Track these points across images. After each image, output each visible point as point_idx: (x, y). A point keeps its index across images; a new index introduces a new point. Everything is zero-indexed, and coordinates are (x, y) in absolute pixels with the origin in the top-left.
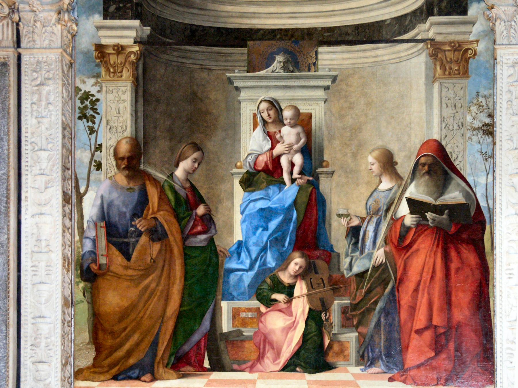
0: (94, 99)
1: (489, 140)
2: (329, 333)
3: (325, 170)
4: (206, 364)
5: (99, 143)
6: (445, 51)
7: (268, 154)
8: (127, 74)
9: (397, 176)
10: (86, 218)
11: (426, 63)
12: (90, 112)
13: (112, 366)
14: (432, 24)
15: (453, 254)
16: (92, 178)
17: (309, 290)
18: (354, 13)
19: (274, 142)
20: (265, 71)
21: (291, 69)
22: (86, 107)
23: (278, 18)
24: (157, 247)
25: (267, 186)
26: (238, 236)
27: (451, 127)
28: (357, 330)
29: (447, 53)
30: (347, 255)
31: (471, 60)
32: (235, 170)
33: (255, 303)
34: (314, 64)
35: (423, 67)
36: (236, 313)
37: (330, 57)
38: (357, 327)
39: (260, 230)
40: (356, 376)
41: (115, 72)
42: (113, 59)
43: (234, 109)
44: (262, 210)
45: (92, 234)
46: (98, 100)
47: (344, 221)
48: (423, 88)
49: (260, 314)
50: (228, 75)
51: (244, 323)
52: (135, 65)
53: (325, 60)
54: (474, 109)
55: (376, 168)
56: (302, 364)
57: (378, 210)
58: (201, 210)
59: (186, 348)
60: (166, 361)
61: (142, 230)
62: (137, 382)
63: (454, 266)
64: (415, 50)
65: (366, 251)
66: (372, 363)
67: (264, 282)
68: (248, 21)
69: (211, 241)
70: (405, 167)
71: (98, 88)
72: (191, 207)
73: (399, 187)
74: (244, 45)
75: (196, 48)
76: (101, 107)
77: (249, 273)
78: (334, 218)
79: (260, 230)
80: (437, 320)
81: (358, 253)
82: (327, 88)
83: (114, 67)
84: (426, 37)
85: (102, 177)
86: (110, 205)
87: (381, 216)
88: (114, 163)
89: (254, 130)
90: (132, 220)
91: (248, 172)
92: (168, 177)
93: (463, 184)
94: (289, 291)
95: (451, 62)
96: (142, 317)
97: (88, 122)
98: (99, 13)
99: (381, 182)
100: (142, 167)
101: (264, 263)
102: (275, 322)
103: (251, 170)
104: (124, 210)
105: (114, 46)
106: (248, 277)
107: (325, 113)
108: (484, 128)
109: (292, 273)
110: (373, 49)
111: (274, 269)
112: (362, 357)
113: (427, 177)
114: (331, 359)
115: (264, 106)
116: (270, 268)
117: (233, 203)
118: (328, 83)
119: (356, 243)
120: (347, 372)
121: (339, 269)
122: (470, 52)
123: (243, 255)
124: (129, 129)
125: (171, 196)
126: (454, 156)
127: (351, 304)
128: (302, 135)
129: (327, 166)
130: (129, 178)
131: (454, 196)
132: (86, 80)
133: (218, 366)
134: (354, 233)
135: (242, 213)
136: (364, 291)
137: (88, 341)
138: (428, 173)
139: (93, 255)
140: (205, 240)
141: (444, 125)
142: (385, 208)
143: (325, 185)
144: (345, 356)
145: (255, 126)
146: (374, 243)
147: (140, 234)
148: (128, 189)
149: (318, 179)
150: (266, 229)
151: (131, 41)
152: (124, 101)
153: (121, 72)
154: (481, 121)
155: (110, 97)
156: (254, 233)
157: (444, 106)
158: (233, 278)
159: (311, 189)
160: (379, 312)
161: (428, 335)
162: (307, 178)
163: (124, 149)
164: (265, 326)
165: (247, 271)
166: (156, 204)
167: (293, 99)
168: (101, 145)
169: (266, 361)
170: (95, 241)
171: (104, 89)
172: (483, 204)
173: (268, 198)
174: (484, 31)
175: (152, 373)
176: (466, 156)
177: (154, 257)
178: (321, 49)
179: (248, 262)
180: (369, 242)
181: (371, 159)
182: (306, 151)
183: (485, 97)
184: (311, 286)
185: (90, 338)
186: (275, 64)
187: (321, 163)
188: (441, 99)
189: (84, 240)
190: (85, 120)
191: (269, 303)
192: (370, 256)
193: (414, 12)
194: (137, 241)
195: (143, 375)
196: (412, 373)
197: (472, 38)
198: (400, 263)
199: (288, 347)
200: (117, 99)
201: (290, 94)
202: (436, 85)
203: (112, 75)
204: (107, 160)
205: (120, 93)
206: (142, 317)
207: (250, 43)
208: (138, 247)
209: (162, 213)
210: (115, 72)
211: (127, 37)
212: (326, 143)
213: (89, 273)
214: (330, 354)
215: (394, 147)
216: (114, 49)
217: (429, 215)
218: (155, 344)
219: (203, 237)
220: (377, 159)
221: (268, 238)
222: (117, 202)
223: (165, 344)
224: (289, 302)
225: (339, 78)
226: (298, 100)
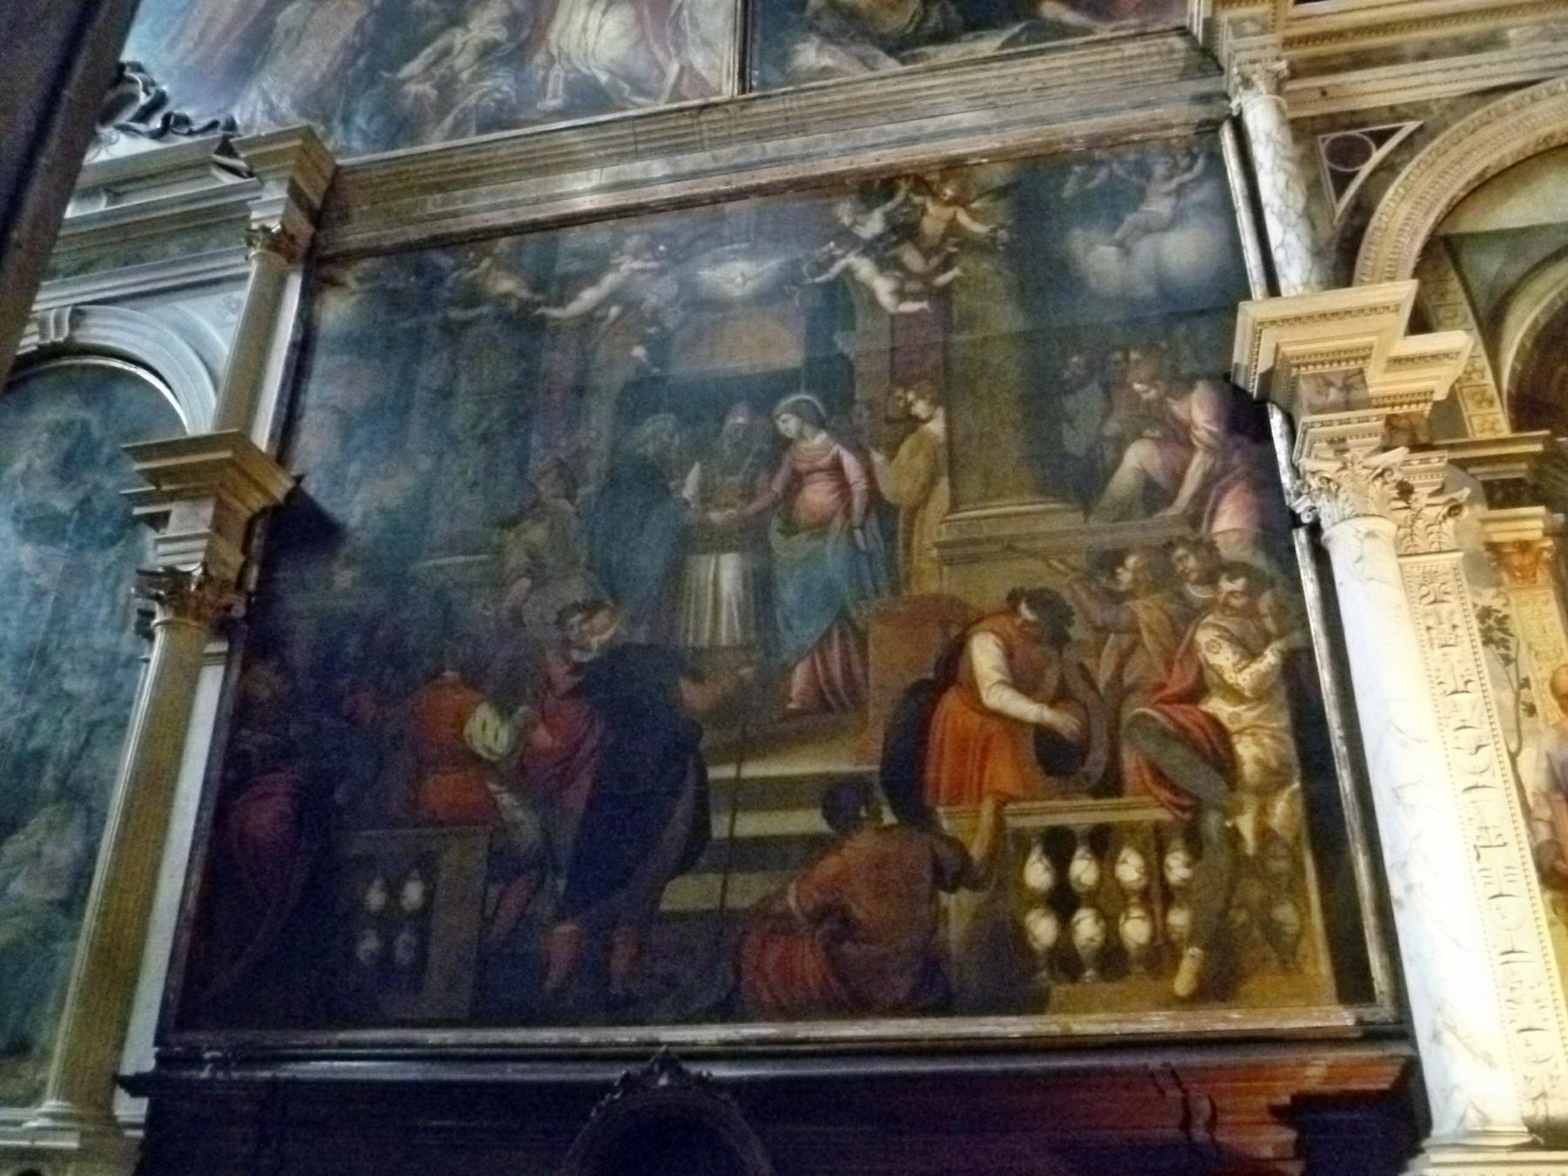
5: (1523, 676)
8: (1543, 576)
10: (1529, 790)
12: (1498, 635)
16: (1524, 728)
22: (1490, 629)
41: (1523, 577)
42: (1516, 560)
45: (1546, 813)
46: (1506, 617)
52: (1554, 566)
76: (1515, 626)
85: (1541, 725)
88: (1555, 704)
98: (1480, 502)
132: (1480, 590)
139: (1555, 848)
151: (1538, 534)
152: (1550, 615)
155: (1526, 611)
170: (1552, 825)
171: (1513, 601)
190: (1493, 647)
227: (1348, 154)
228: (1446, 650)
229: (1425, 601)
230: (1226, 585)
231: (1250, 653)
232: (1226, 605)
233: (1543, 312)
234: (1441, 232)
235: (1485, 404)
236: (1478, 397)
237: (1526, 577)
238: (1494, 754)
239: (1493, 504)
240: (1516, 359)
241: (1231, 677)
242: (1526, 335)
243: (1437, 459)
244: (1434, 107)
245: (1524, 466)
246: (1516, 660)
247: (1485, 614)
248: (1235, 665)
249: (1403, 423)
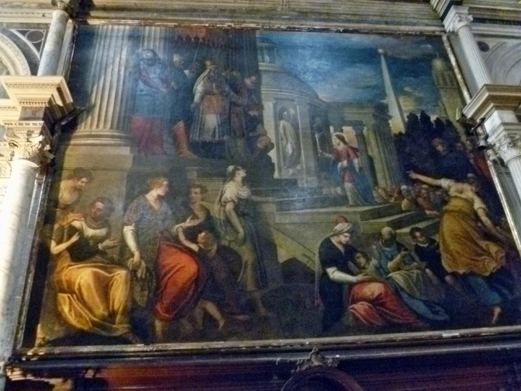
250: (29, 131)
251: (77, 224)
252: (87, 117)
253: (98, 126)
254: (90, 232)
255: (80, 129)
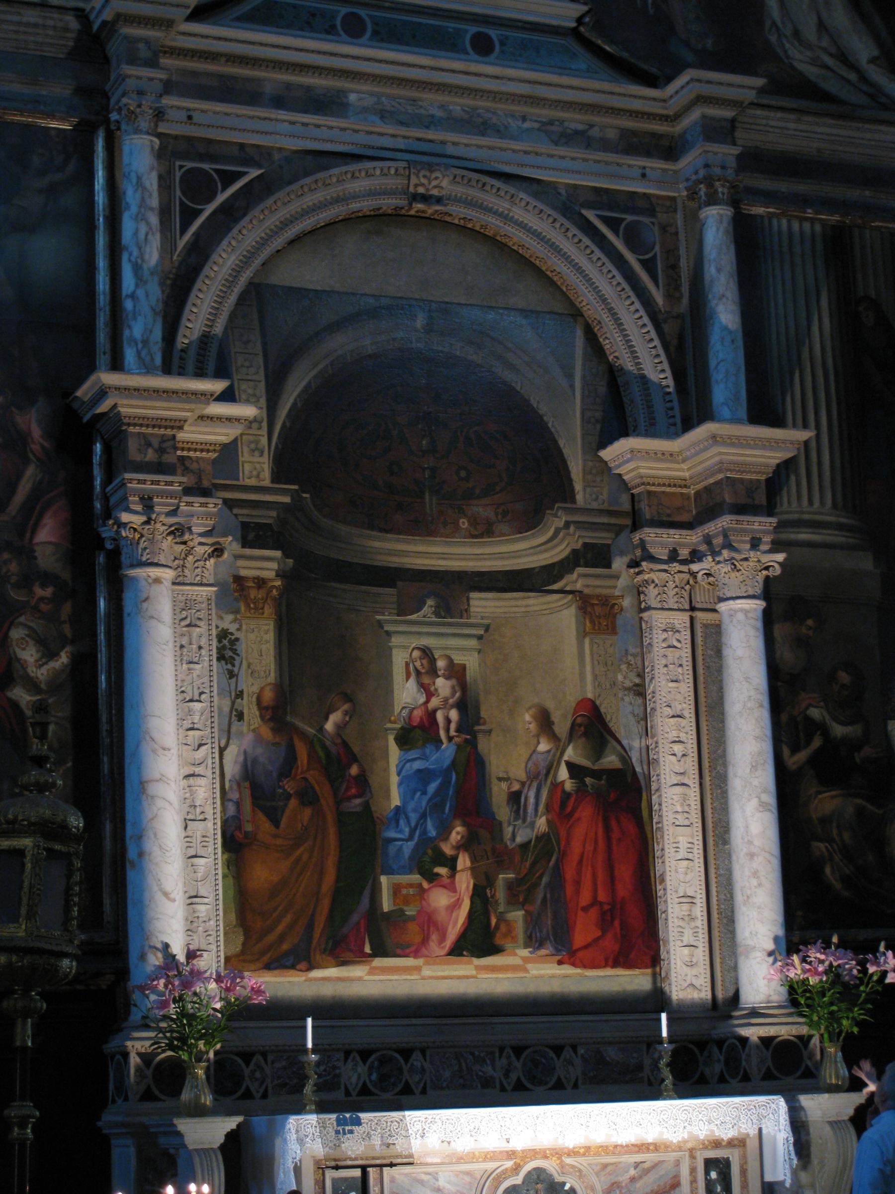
0: (233, 637)
1: (639, 701)
2: (495, 911)
3: (482, 727)
4: (367, 949)
5: (239, 689)
6: (593, 604)
7: (423, 708)
8: (268, 610)
9: (553, 737)
10: (228, 776)
11: (576, 616)
12: (229, 653)
13: (263, 953)
14: (580, 576)
15: (613, 823)
16: (234, 729)
17: (472, 863)
18: (503, 558)
19: (429, 695)
20: (416, 615)
21: (443, 614)
23: (427, 558)
24: (307, 812)
25: (424, 746)
26: (396, 801)
27: (604, 686)
28: (523, 906)
29: (596, 607)
30: (509, 824)
31: (618, 616)
32: (389, 725)
33: (416, 878)
34: (466, 611)
35: (573, 619)
36: (396, 890)
37: (483, 605)
38: (523, 905)
39: (418, 794)
40: (525, 960)
41: (256, 608)
42: (253, 593)
43: (386, 656)
44: (419, 771)
45: (235, 796)
46: (237, 639)
47: (504, 786)
48: (574, 641)
49: (422, 891)
50: (379, 617)
51: (406, 900)
52: (278, 602)
53: (477, 607)
54: (624, 667)
55: (533, 727)
56: (470, 947)
57: (539, 774)
58: (354, 770)
59: (345, 930)
60: (323, 947)
61: (291, 792)
62: (292, 972)
63: (616, 834)
64: (565, 601)
65: (529, 819)
66: (540, 945)
67: (426, 853)
68: (396, 559)
69: (367, 806)
70: (562, 727)
71: (237, 626)
72: (343, 767)
73: (557, 749)
74: (392, 585)
75: (343, 586)
76: (242, 647)
77: (409, 843)
78: (494, 781)
79: (418, 794)
80: (602, 896)
81: (520, 822)
82: (480, 638)
83: (254, 603)
84: (574, 589)
85: (245, 729)
86: (255, 761)
87: (541, 781)
88: (257, 713)
89: (407, 681)
90: (280, 781)
91: (402, 728)
92: (317, 731)
93: (619, 748)
94: (451, 863)
95: (599, 617)
96: (295, 895)
97: (226, 664)
99: (539, 743)
100: (288, 718)
101: (424, 832)
102: (440, 899)
103: (406, 726)
104: (270, 768)
105: (254, 578)
106: (408, 848)
107: (480, 665)
108: (635, 688)
109: (454, 844)
110: (524, 598)
111: (435, 838)
112: (530, 937)
113: (584, 739)
114: (498, 941)
115: (416, 654)
116: (430, 838)
117: (388, 762)
118: (482, 632)
119: (517, 811)
120: (516, 955)
121: (502, 839)
122: (616, 607)
123: (402, 822)
124: (273, 674)
125: (321, 754)
126: (609, 717)
127: (516, 879)
128: (457, 688)
129: (484, 724)
130: (275, 731)
131: (611, 760)
132: (224, 615)
133: (380, 951)
134: (515, 798)
135: (399, 774)
136: (528, 864)
137: (234, 923)
138: (586, 734)
140: (360, 805)
141: (597, 683)
142: (545, 772)
143: (483, 745)
144: (513, 938)
145: (408, 677)
146: (536, 810)
147: (288, 797)
148: (273, 744)
149: (475, 738)
150: (424, 793)
151: (272, 574)
152: (267, 642)
153: (262, 609)
154: (631, 681)
155: (252, 636)
156: (412, 798)
157: (596, 663)
158: (392, 849)
159: (468, 749)
160: (545, 887)
161: (594, 913)
162: (464, 736)
163: (268, 696)
164: (429, 905)
165: (407, 840)
166: (305, 761)
167: (447, 648)
168: (242, 692)
169: (431, 944)
170: (238, 804)
171: (244, 627)
172: (638, 769)
173: (424, 757)
174: (628, 586)
175: (309, 962)
176: (621, 716)
177: (305, 824)
178: (473, 595)
179: (407, 830)
180: (531, 809)
181: (527, 717)
182: (462, 706)
183: (633, 655)
184: (474, 859)
185: (237, 919)
186: (426, 608)
187: (478, 720)
188: (592, 654)
189: (226, 803)
190: (223, 662)
191: (432, 878)
192: (532, 825)
193: (561, 562)
194: (286, 805)
195: (298, 963)
196: (580, 954)
197: (617, 593)
198: (563, 833)
199: (453, 927)
200: (259, 639)
201: (442, 642)
202: (587, 641)
203: (252, 611)
204: (249, 708)
205: (262, 633)
206: (295, 895)
207: (400, 584)
208: (288, 812)
209: (312, 772)
210: (256, 608)
211: (268, 569)
212: (482, 698)
213: (235, 843)
214: (498, 935)
215: (550, 705)
216: (254, 583)
217: (588, 780)
218: (310, 926)
219: (358, 801)
220: (532, 716)
221: (427, 804)
222: (261, 759)
223: (322, 925)
224: (452, 876)
225: (492, 627)
226: (451, 649)
227: (198, 187)
228: (192, 666)
229: (184, 623)
230: (39, 592)
231: (50, 654)
232: (36, 608)
233: (315, 377)
234: (256, 280)
235: (257, 453)
236: (253, 446)
237: (257, 609)
238: (210, 751)
239: (245, 544)
240: (289, 415)
241: (32, 670)
242: (299, 396)
243: (213, 505)
244: (276, 156)
245: (274, 514)
246: (237, 676)
247: (223, 635)
248: (36, 661)
249: (195, 466)
250: (753, 538)
251: (815, 713)
252: (788, 476)
253: (810, 502)
254: (838, 730)
255: (781, 505)
